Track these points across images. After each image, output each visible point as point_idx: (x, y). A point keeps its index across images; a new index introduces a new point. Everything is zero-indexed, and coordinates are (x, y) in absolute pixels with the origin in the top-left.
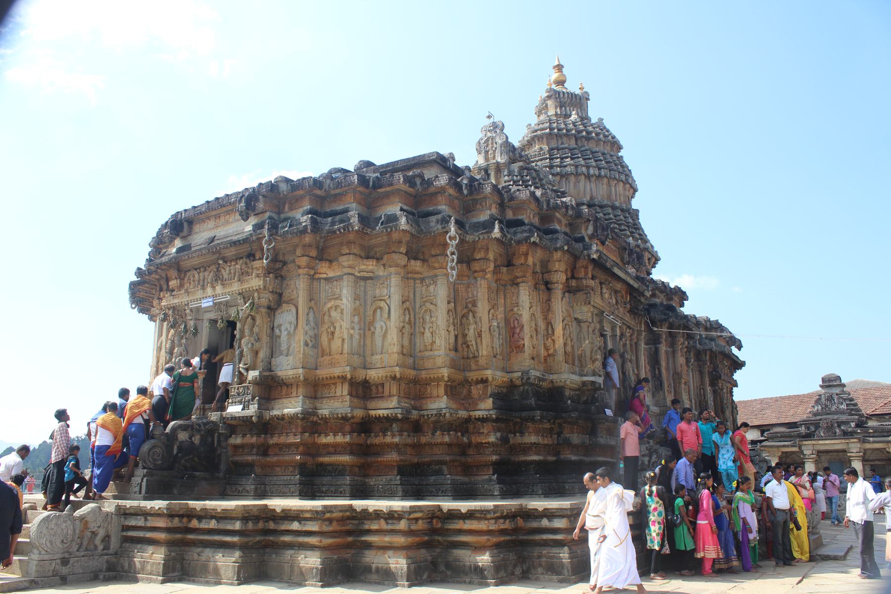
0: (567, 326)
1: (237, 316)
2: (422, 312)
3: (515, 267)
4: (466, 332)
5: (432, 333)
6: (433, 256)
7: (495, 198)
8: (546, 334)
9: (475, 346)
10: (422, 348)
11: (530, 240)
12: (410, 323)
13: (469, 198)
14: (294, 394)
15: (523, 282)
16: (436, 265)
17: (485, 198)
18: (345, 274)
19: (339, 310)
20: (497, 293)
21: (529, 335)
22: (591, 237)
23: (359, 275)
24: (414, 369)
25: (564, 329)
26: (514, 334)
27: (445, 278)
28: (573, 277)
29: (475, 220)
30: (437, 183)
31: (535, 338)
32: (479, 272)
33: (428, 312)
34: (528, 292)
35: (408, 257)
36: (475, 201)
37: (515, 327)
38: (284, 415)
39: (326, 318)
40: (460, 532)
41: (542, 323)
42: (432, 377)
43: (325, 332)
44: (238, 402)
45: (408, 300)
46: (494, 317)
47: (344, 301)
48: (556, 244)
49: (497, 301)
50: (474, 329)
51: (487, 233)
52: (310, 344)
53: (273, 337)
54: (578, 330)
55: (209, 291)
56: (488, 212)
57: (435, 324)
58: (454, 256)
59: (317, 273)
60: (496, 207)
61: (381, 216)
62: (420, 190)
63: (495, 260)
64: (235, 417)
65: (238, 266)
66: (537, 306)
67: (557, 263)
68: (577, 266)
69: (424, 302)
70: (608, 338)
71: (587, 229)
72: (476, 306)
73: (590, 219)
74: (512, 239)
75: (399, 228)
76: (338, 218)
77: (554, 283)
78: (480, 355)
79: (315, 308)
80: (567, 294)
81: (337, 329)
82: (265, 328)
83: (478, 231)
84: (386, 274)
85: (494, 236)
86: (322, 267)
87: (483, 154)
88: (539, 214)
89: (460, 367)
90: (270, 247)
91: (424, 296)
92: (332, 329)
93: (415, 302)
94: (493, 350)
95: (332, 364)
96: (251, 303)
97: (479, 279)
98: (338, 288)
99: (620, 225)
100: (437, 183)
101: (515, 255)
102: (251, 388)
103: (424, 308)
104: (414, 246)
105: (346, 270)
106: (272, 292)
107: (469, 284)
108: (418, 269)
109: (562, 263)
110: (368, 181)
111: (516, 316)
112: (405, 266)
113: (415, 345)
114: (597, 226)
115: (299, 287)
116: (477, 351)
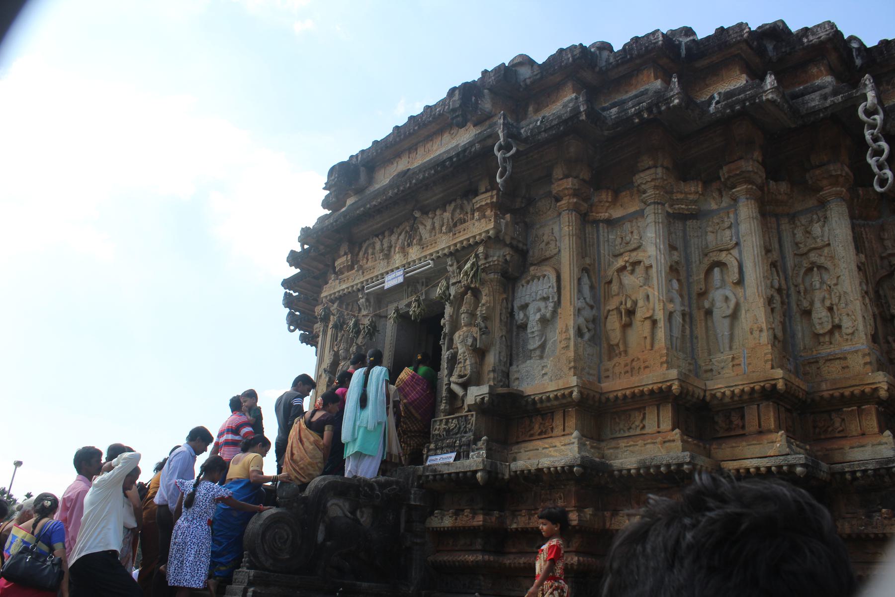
1: (447, 293)
5: (830, 309)
14: (558, 431)
38: (541, 470)
42: (847, 393)
44: (448, 446)
47: (651, 250)
52: (587, 336)
55: (398, 259)
64: (442, 475)
65: (447, 215)
81: (641, 303)
82: (498, 312)
90: (508, 155)
95: (631, 371)
96: (473, 264)
102: (474, 419)
106: (511, 246)
113: (793, 336)
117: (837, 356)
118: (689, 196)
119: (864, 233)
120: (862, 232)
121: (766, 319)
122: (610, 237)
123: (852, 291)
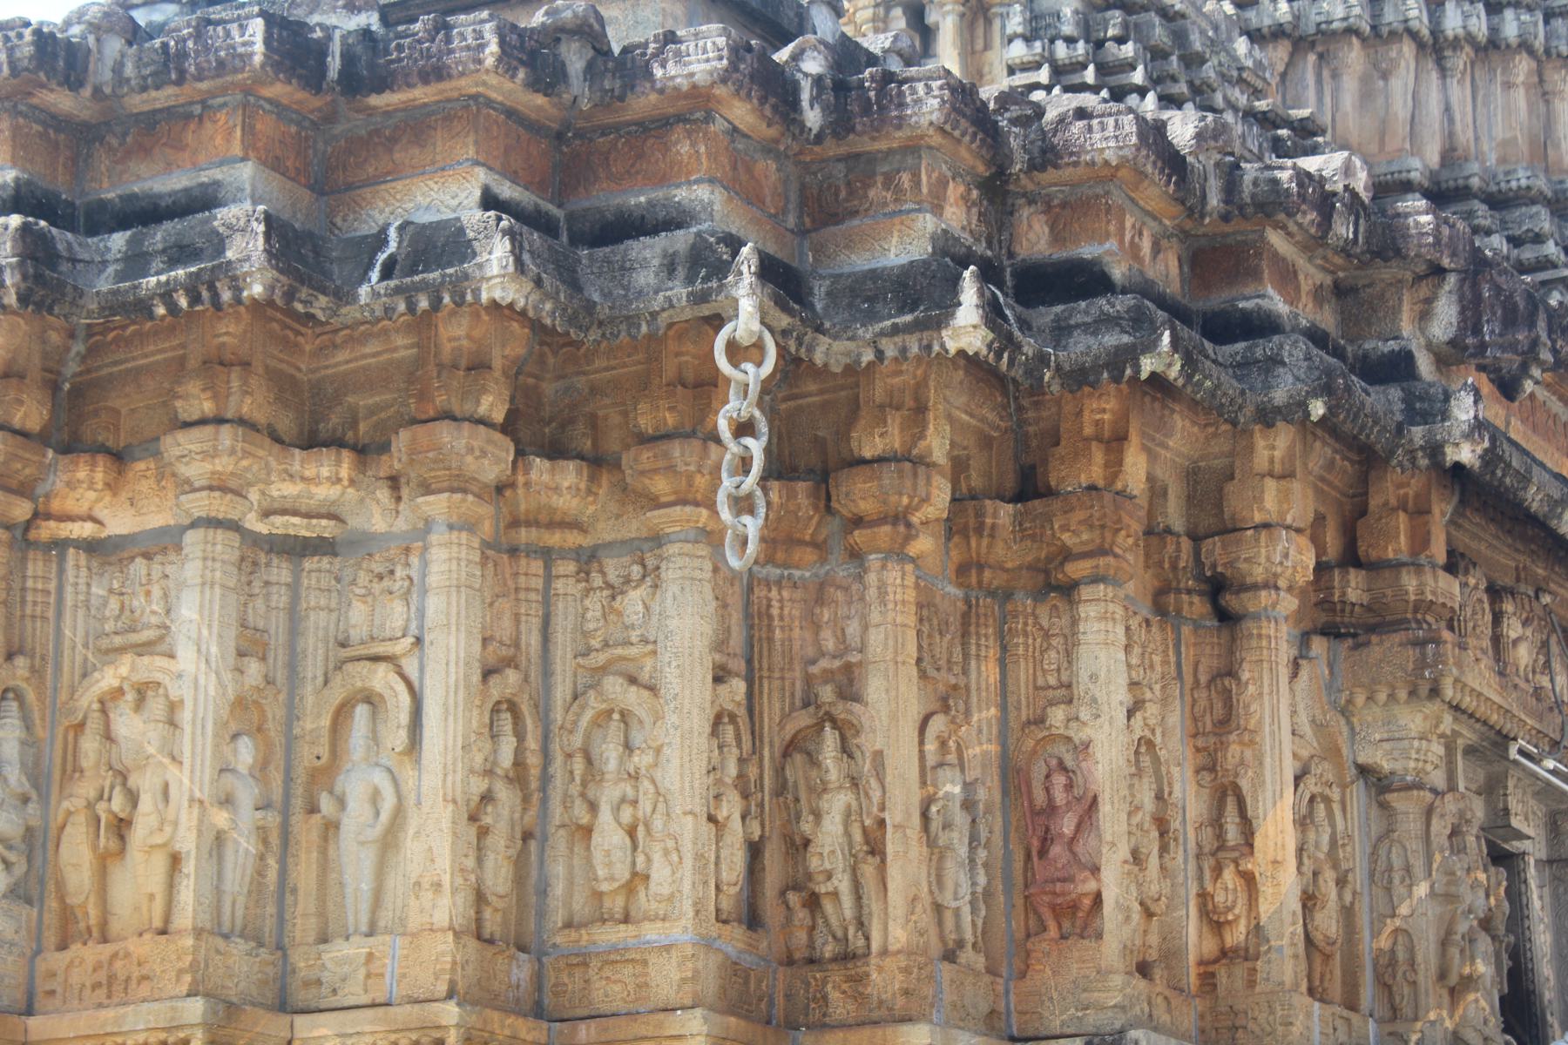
0: (1321, 808)
2: (585, 721)
3: (1056, 504)
4: (806, 827)
5: (631, 832)
6: (644, 440)
7: (964, 153)
8: (1209, 843)
9: (847, 902)
10: (576, 907)
11: (1137, 368)
13: (832, 148)
15: (1096, 579)
16: (661, 486)
17: (913, 148)
18: (194, 525)
19: (156, 706)
20: (965, 634)
21: (1124, 852)
22: (1450, 356)
23: (262, 528)
24: (538, 1011)
25: (1303, 822)
26: (1046, 841)
27: (703, 550)
28: (1352, 558)
29: (860, 261)
30: (672, 70)
31: (1154, 862)
32: (882, 520)
33: (615, 726)
34: (1120, 630)
35: (517, 442)
36: (862, 167)
37: (1051, 809)
39: (90, 745)
41: (1192, 789)
43: (81, 819)
45: (511, 662)
46: (950, 755)
47: (187, 658)
48: (1268, 387)
49: (965, 672)
50: (848, 814)
51: (917, 326)
54: (1375, 830)
56: (927, 223)
57: (646, 784)
58: (749, 441)
59: (48, 516)
60: (965, 198)
61: (384, 230)
62: (585, 105)
63: (959, 467)
66: (1165, 702)
67: (1271, 485)
68: (1375, 502)
69: (595, 670)
70: (1532, 872)
71: (1425, 315)
72: (857, 698)
73: (1446, 262)
74: (1042, 359)
75: (476, 292)
76: (160, 236)
77: (1255, 587)
78: (875, 946)
79: (31, 696)
80: (1319, 646)
81: (146, 803)
83: (871, 317)
84: (401, 525)
85: (952, 347)
86: (73, 486)
88: (1184, 235)
89: (771, 1003)
91: (595, 643)
92: (118, 804)
93: (547, 672)
94: (940, 923)
97: (874, 559)
98: (156, 592)
100: (672, 70)
101: (1057, 444)
103: (594, 704)
104: (549, 388)
105: (200, 504)
107: (822, 586)
108: (566, 503)
109: (1296, 486)
110: (321, 50)
111: (1061, 750)
112: (500, 489)
113: (543, 891)
114: (1477, 298)
116: (860, 924)
117: (628, 956)
118: (314, 489)
119: (775, 604)
120: (769, 600)
121: (453, 861)
122: (94, 590)
123: (682, 789)
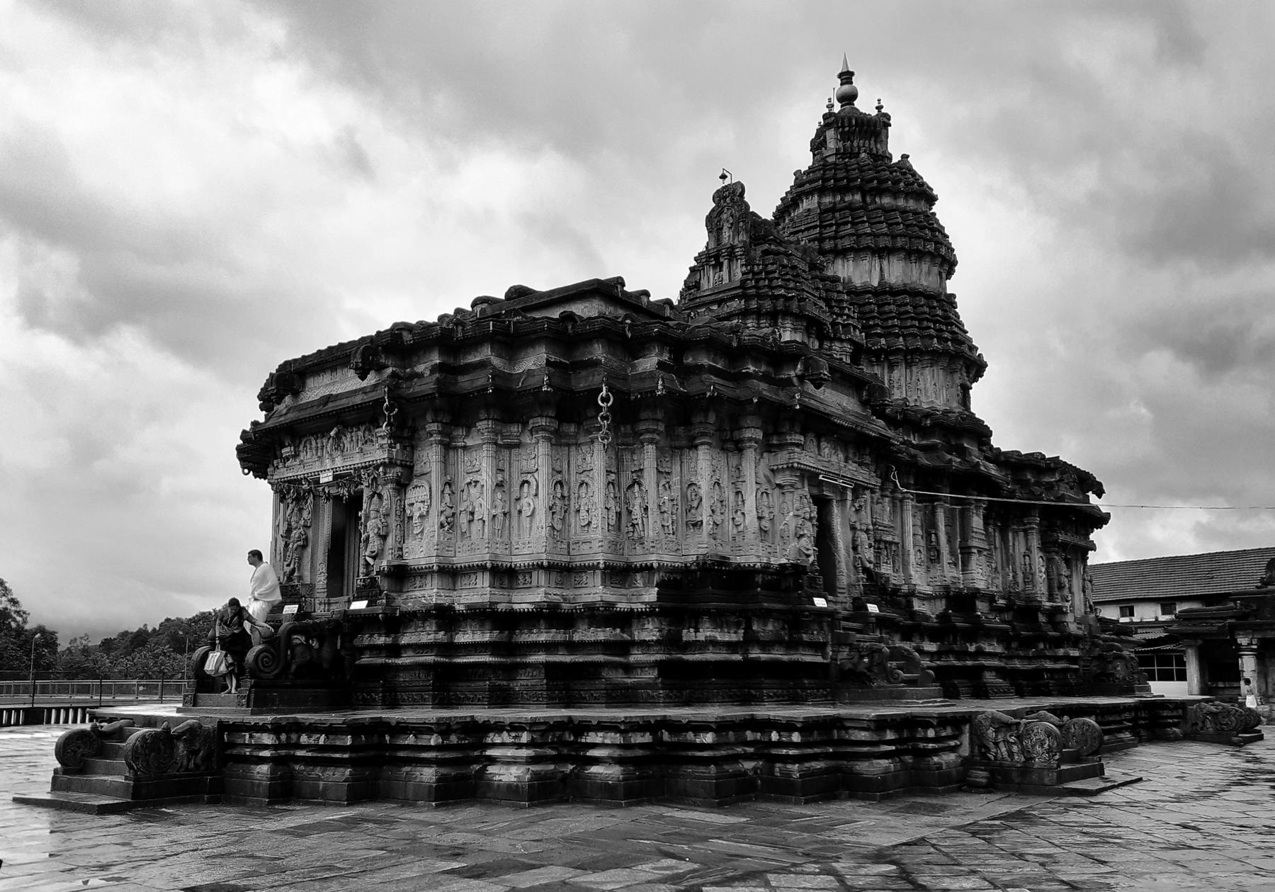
12: (563, 497)
14: (428, 586)
19: (479, 485)
23: (501, 443)
40: (594, 746)
47: (484, 474)
53: (405, 519)
54: (781, 500)
55: (328, 464)
65: (360, 433)
80: (765, 455)
87: (715, 234)
99: (920, 321)
106: (401, 465)
115: (430, 458)
